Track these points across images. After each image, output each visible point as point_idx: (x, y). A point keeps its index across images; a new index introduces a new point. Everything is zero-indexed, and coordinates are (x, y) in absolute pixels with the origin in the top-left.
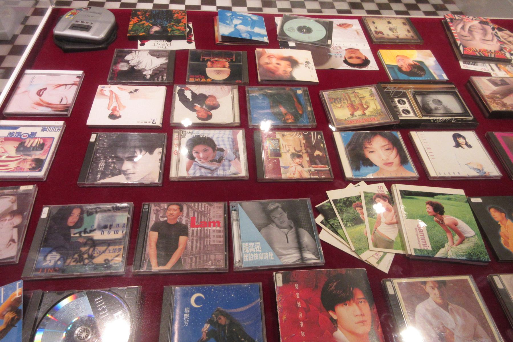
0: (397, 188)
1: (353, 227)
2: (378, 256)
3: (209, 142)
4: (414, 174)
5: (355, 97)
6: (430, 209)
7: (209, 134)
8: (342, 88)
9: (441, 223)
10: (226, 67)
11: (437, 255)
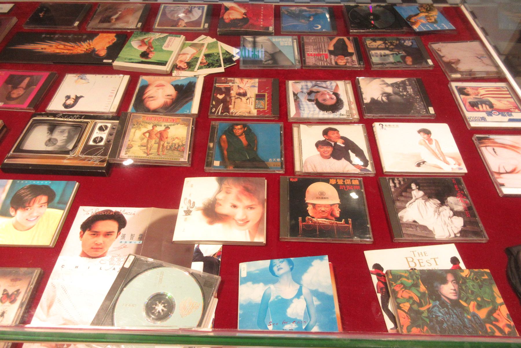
3: (322, 107)
5: (151, 147)
7: (324, 114)
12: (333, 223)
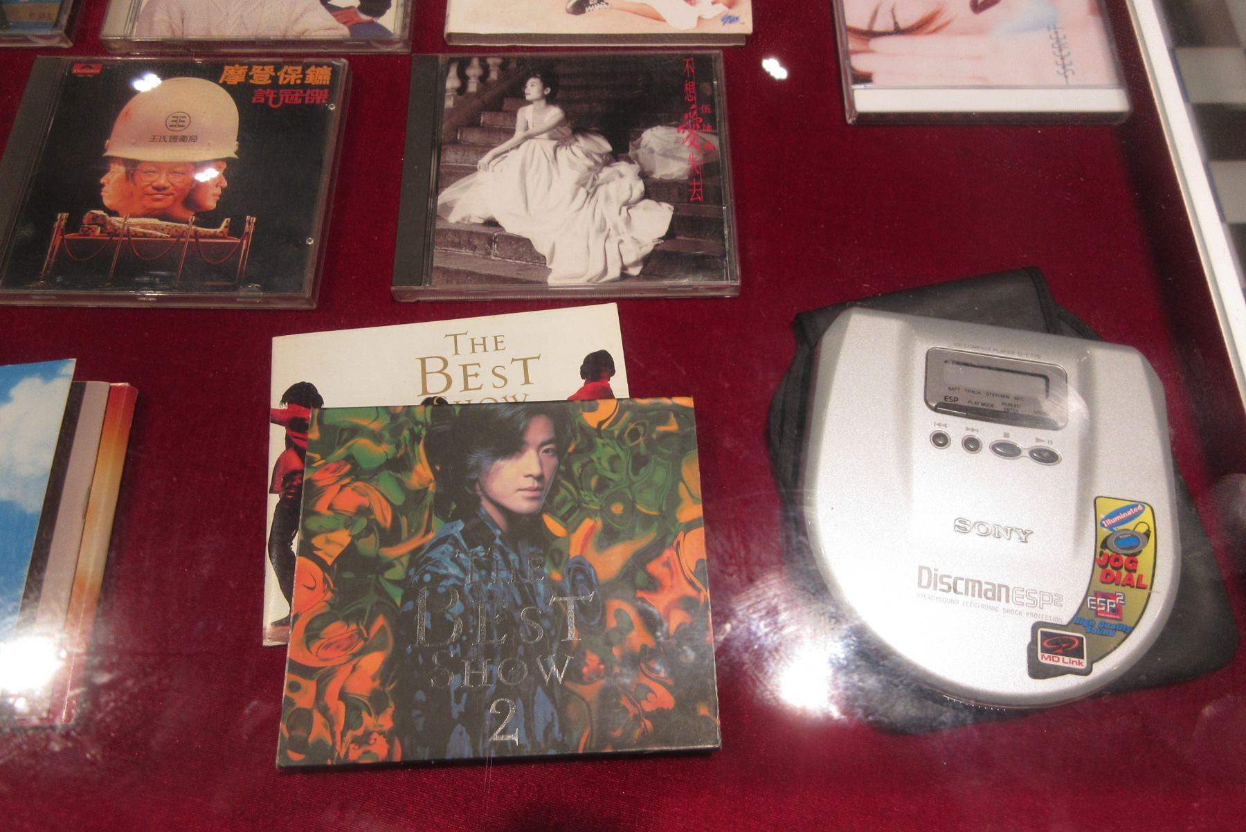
12: (182, 234)
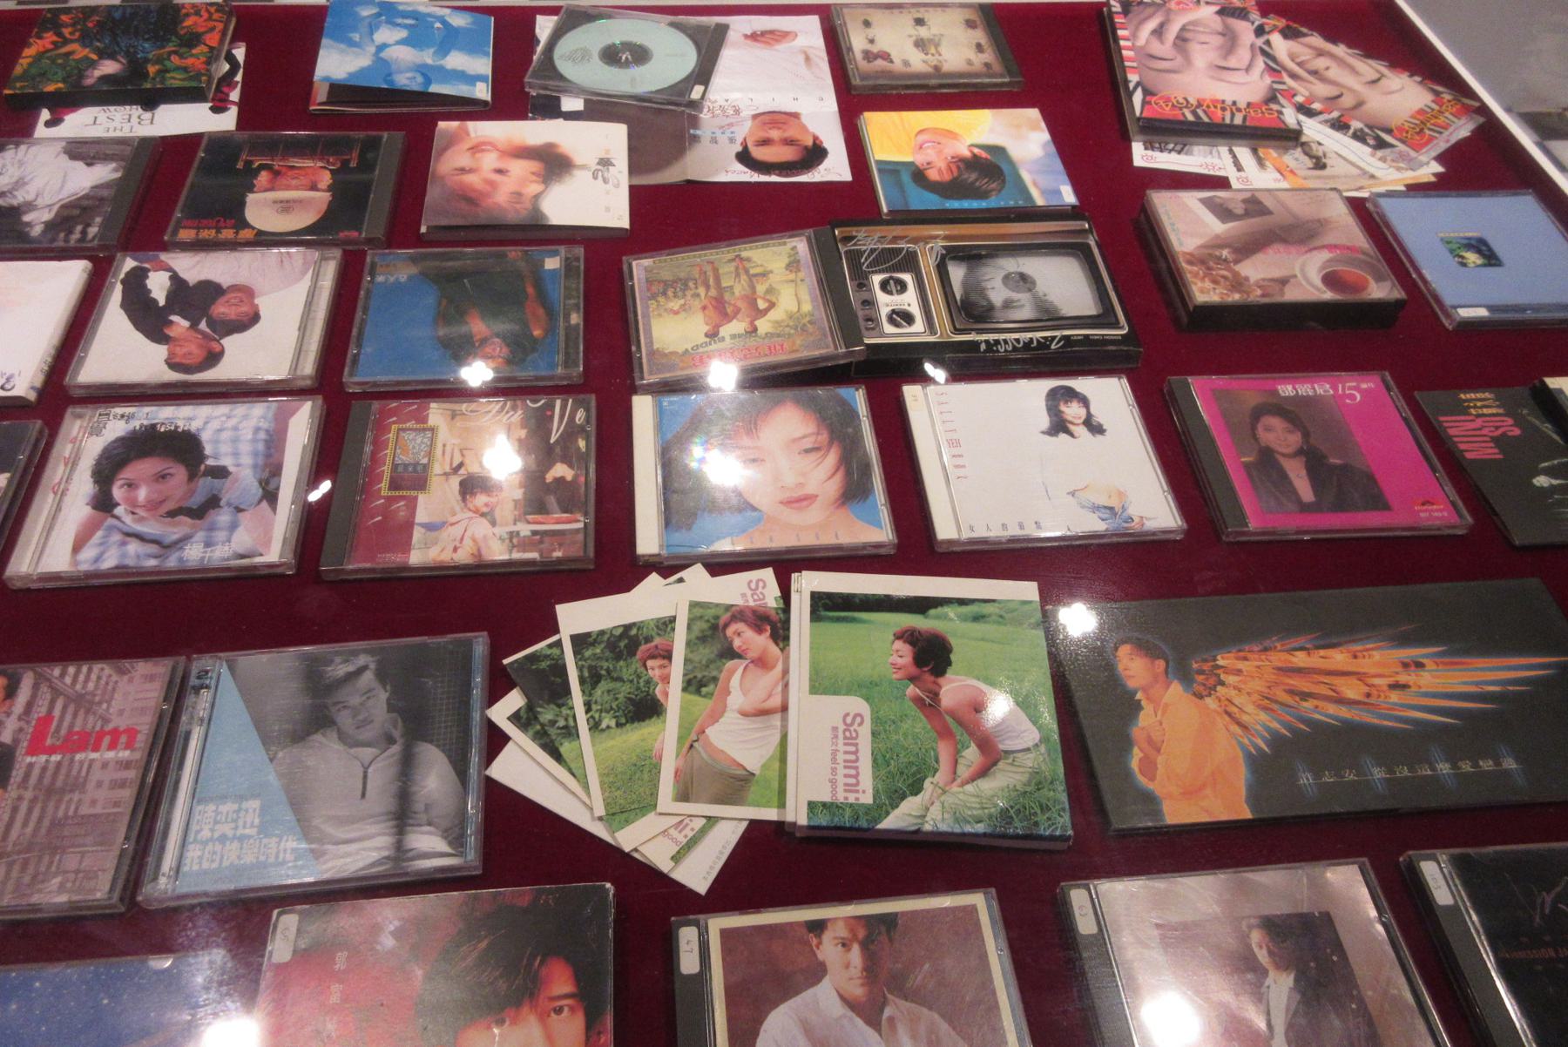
0: (808, 583)
1: (619, 731)
2: (684, 833)
3: (184, 448)
4: (878, 530)
5: (738, 275)
6: (903, 654)
8: (688, 248)
9: (929, 705)
10: (319, 186)
11: (880, 826)
12: (281, 160)
